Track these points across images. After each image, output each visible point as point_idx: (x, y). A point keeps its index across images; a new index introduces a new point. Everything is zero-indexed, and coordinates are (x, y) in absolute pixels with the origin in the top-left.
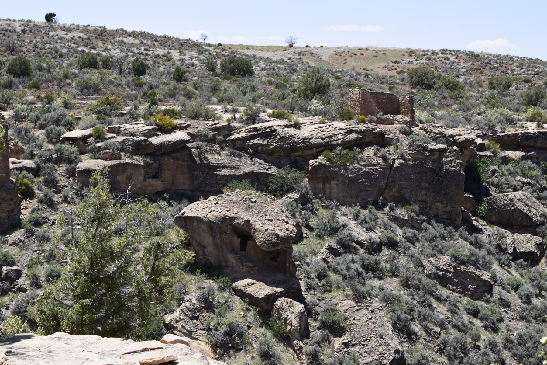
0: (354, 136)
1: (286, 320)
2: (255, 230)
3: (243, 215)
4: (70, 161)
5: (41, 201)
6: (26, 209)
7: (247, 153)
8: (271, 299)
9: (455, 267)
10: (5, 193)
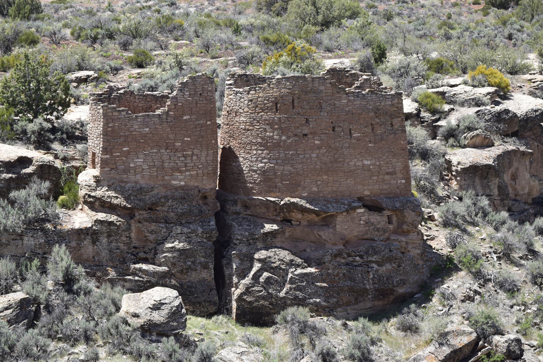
4: (425, 155)
5: (446, 224)
6: (432, 239)
10: (413, 214)
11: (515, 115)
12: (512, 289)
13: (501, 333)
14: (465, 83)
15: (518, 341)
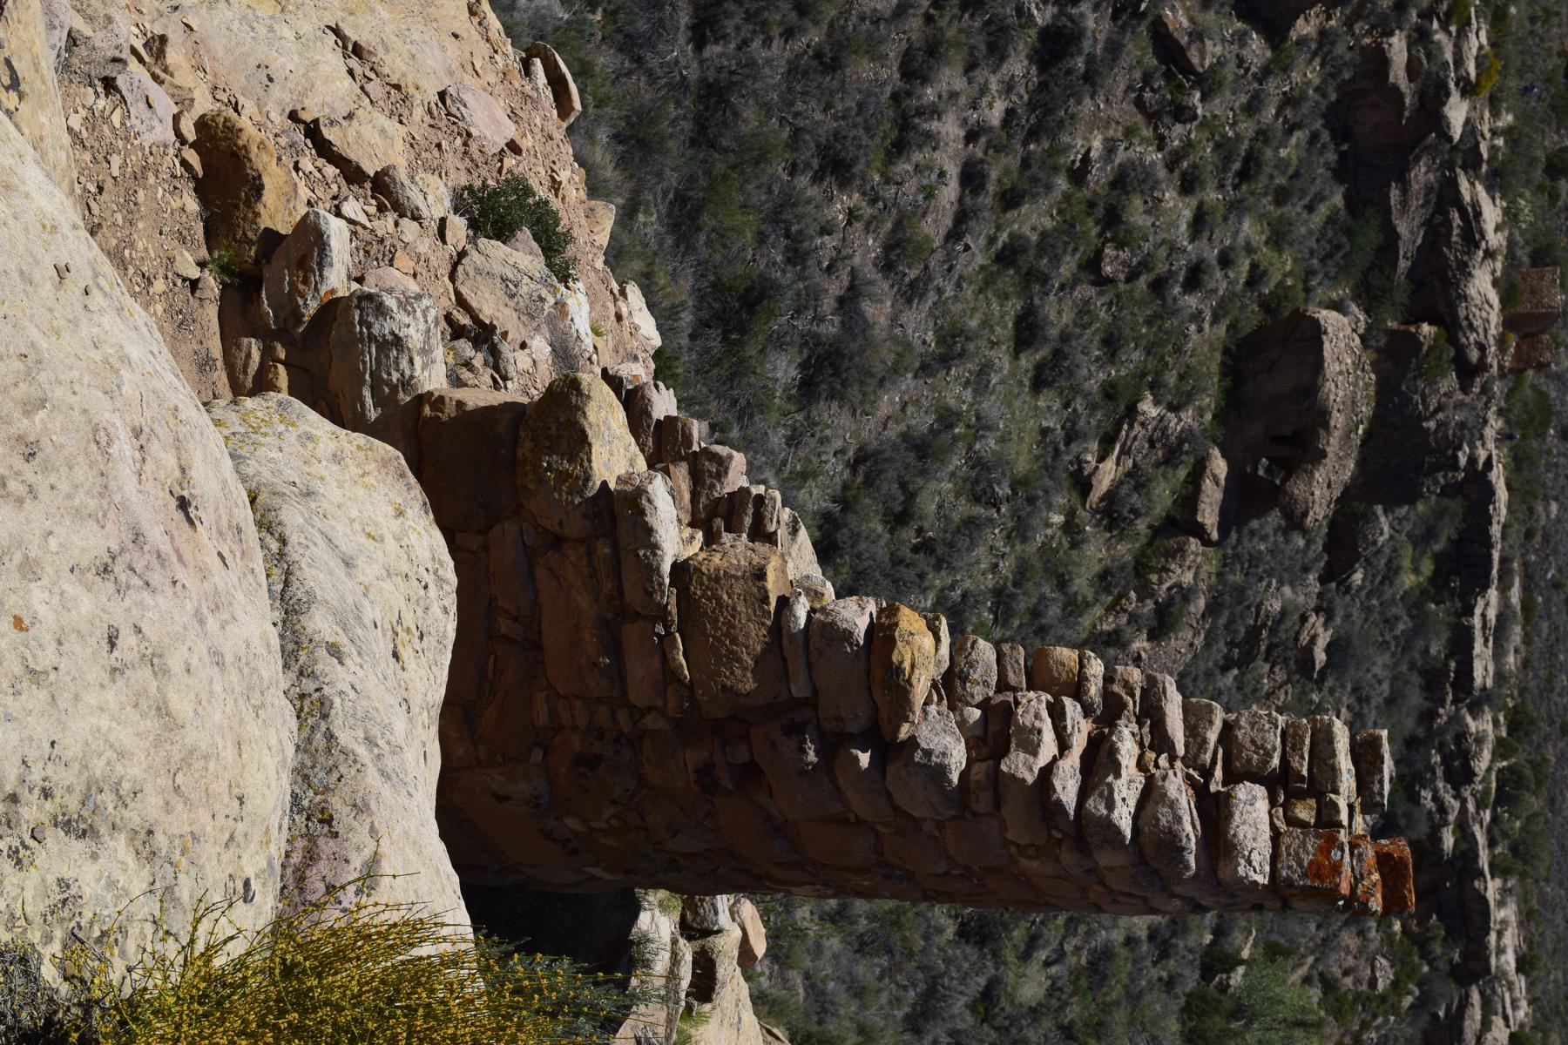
0: (1474, 355)
1: (1167, 570)
2: (1312, 473)
3: (1333, 445)
5: (1323, 33)
7: (1433, 215)
8: (1199, 531)
9: (1264, 625)
11: (1444, 104)
12: (1252, 108)
13: (1203, 100)
14: (1481, 47)
15: (1195, 117)
